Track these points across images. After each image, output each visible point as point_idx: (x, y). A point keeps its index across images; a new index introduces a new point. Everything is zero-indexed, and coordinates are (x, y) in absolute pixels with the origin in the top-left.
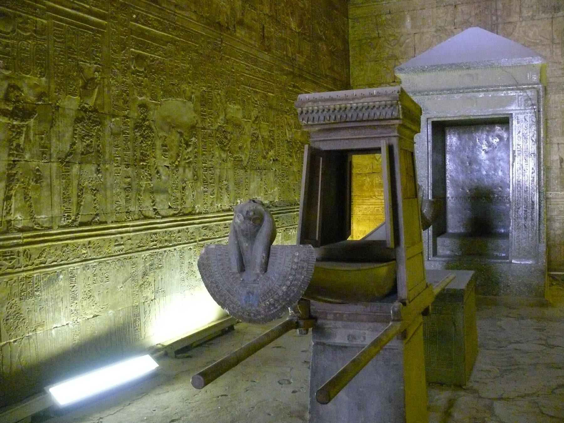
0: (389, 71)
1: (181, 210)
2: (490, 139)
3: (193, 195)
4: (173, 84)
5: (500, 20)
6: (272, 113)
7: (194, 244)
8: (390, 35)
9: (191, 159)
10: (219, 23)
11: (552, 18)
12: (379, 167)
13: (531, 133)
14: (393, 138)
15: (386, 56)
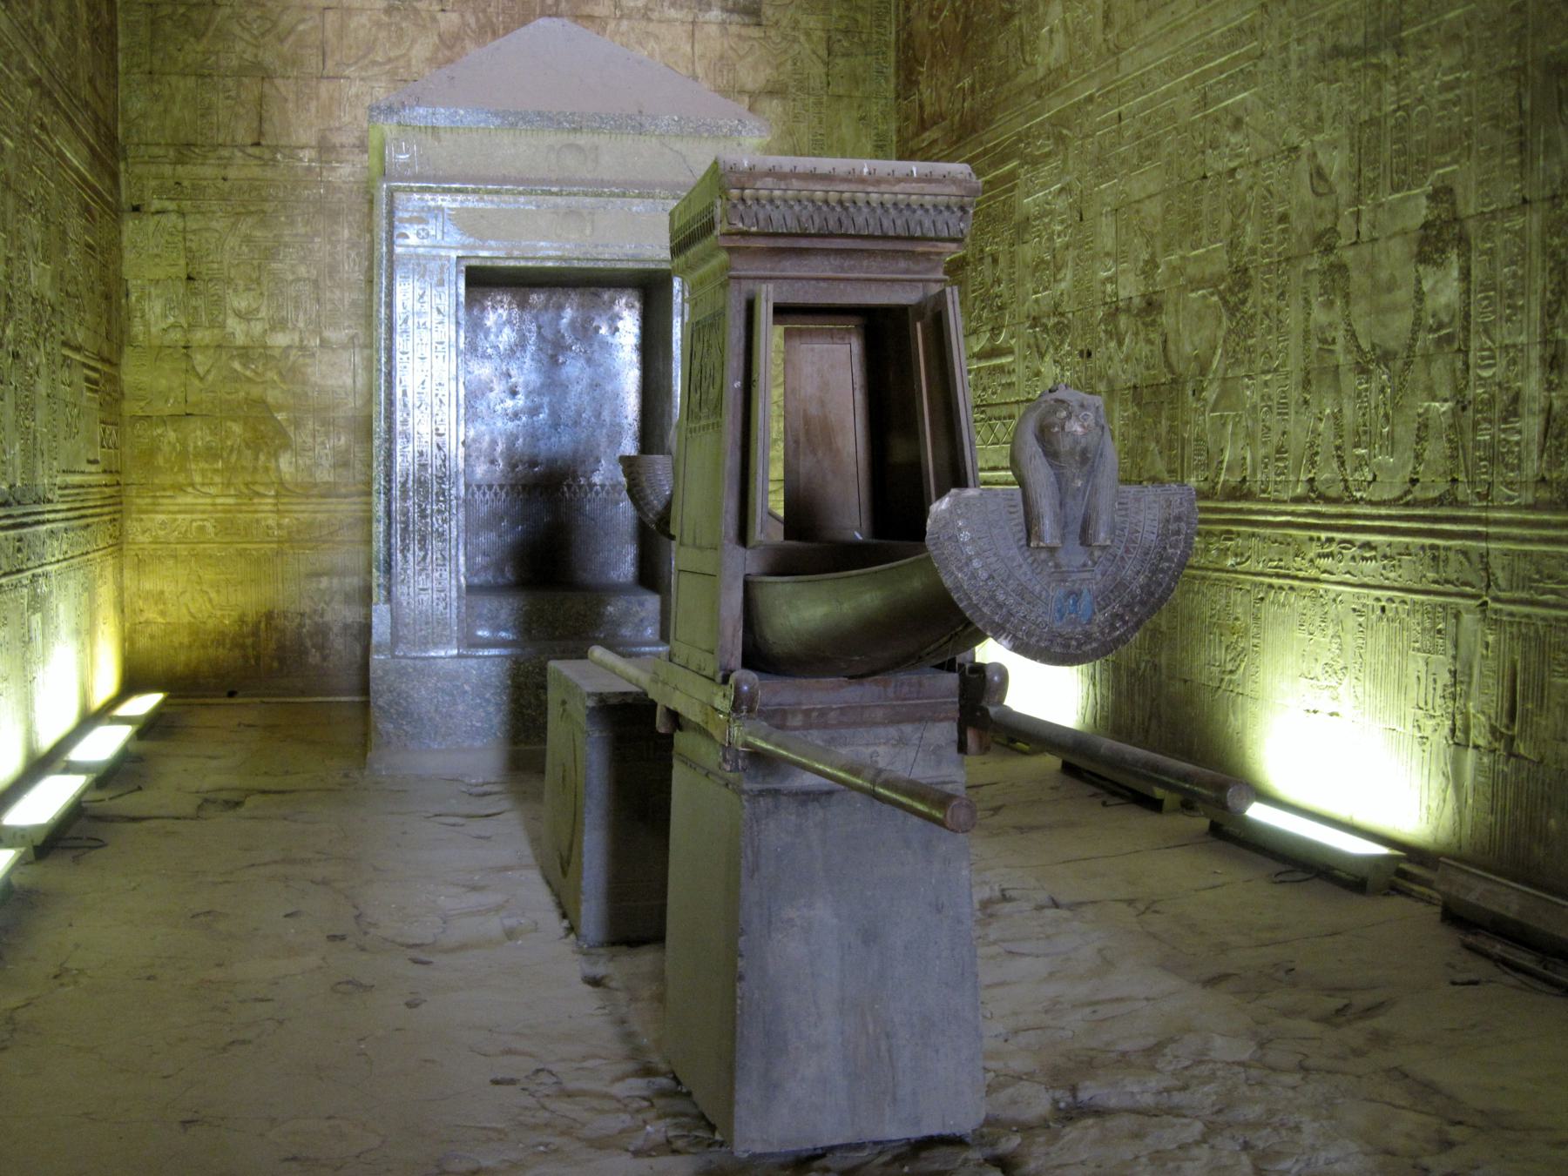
11: (694, 23)
12: (204, 395)
15: (235, 63)
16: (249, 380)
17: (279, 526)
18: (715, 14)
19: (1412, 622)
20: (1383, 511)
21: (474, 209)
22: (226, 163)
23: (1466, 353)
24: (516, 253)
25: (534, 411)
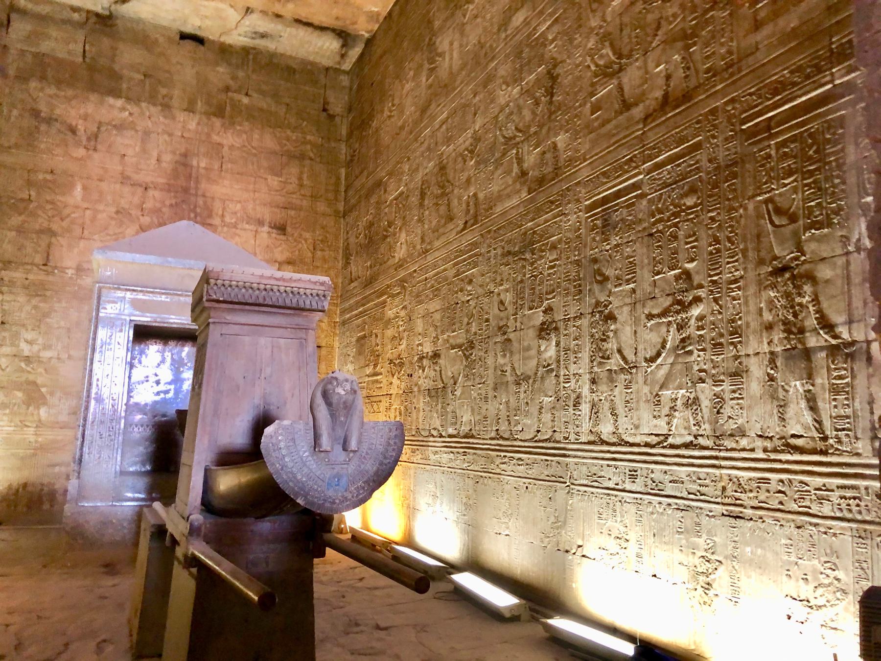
5: (198, 218)
8: (47, 202)
15: (37, 227)
16: (29, 372)
17: (36, 442)
18: (266, 228)
19: (538, 493)
20: (526, 444)
21: (141, 299)
22: (28, 272)
23: (559, 377)
24: (158, 320)
25: (167, 392)
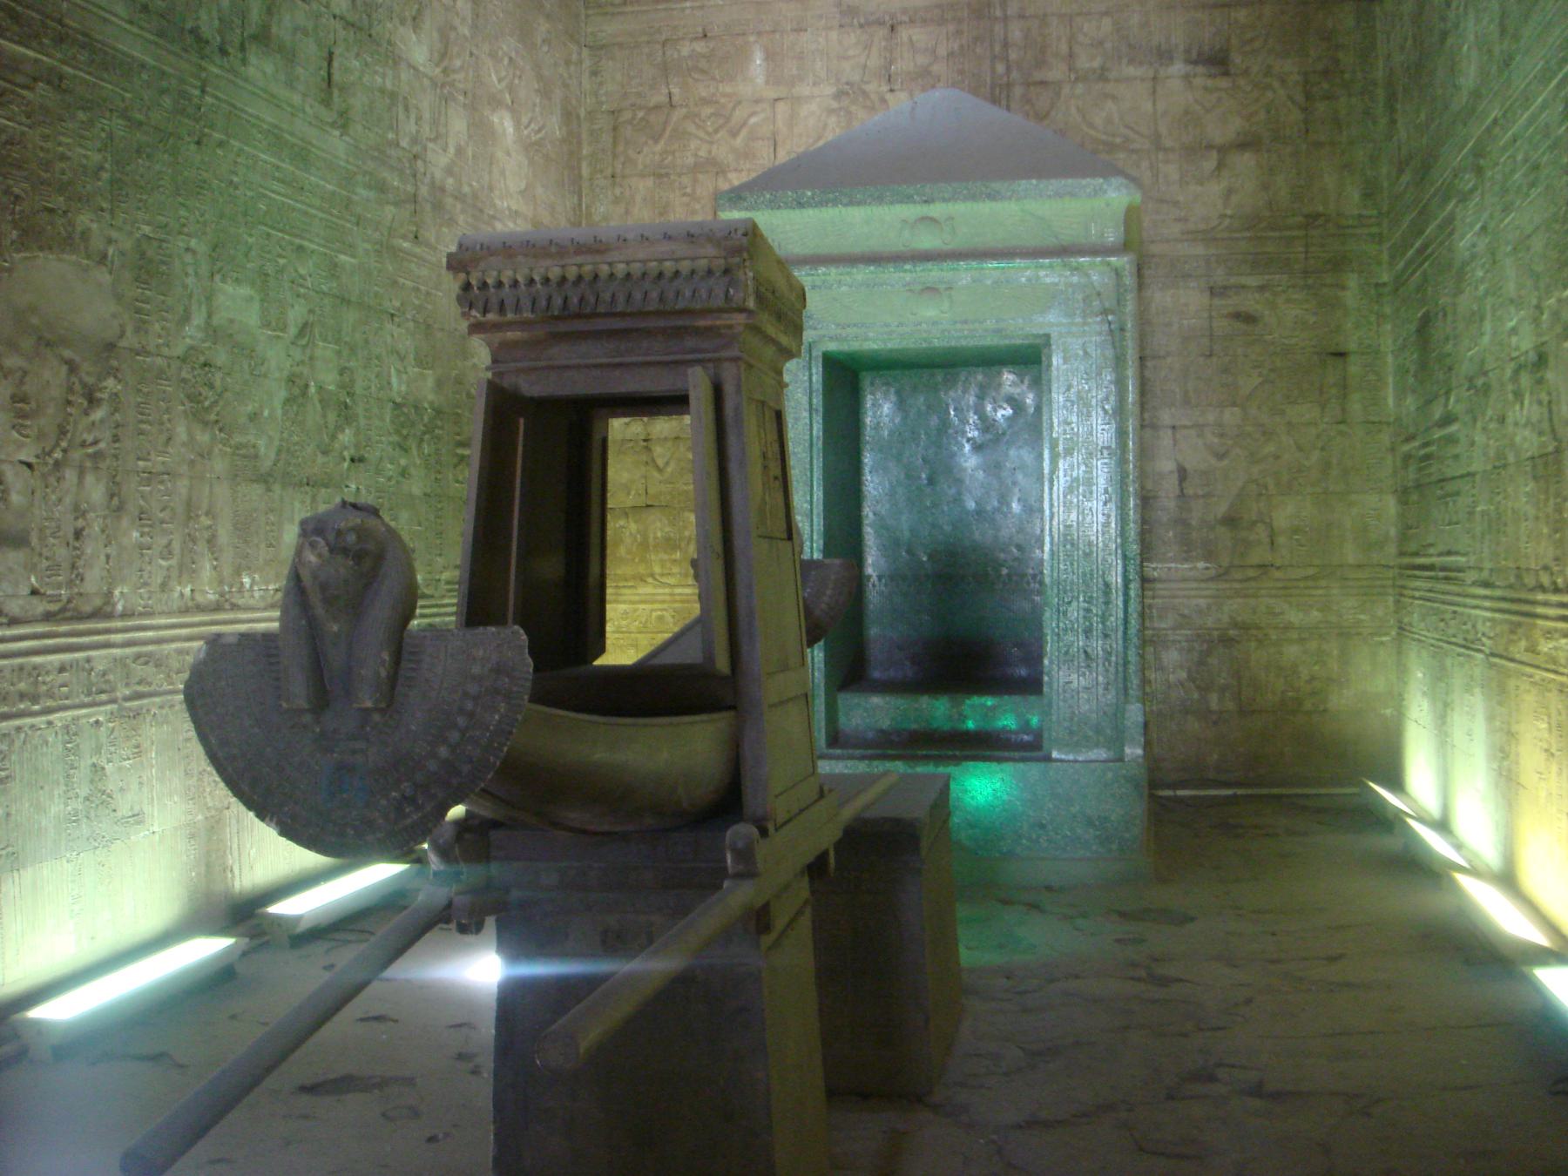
0: (698, 207)
1: (69, 601)
2: (989, 408)
3: (108, 557)
4: (51, 211)
5: (1015, 75)
6: (351, 316)
7: (109, 707)
8: (705, 102)
9: (102, 445)
10: (194, 32)
13: (1100, 392)
14: (726, 365)
15: (690, 160)
18: (1178, 67)
